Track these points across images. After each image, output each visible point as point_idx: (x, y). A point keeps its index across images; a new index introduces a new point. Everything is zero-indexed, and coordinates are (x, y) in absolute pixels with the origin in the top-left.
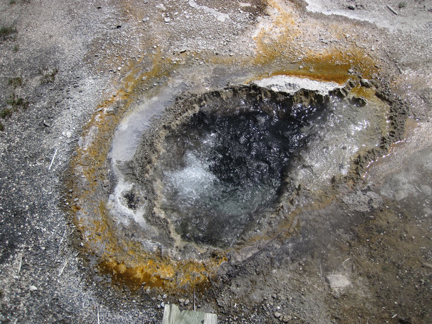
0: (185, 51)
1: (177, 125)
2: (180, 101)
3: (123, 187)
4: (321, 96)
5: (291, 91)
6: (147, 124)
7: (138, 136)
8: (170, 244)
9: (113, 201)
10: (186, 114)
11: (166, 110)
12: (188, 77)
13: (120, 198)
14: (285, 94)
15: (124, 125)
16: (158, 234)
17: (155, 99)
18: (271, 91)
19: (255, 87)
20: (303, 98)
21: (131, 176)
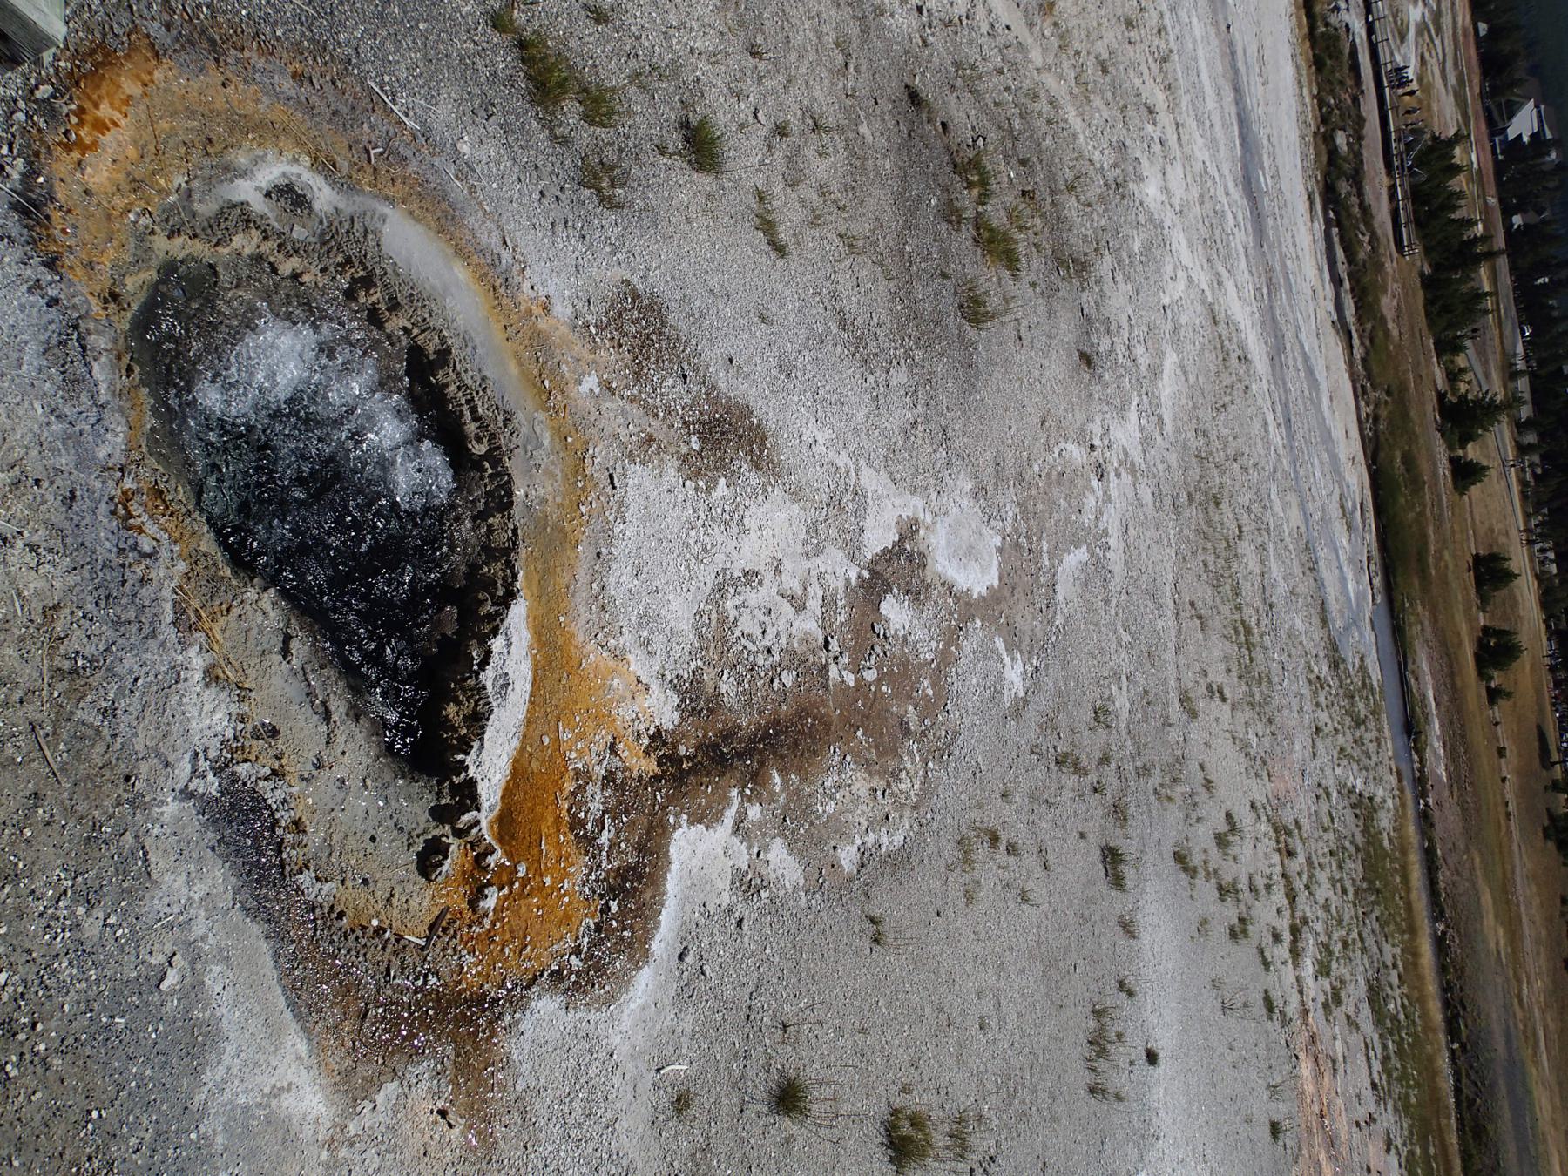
0: (614, 488)
1: (447, 385)
2: (500, 418)
3: (324, 196)
4: (467, 754)
5: (488, 677)
6: (460, 321)
7: (433, 288)
8: (167, 220)
9: (295, 160)
10: (468, 416)
11: (484, 379)
12: (552, 463)
13: (299, 176)
14: (485, 662)
15: (461, 273)
16: (197, 207)
17: (514, 369)
18: (495, 632)
19: (511, 595)
20: (467, 709)
21: (347, 225)
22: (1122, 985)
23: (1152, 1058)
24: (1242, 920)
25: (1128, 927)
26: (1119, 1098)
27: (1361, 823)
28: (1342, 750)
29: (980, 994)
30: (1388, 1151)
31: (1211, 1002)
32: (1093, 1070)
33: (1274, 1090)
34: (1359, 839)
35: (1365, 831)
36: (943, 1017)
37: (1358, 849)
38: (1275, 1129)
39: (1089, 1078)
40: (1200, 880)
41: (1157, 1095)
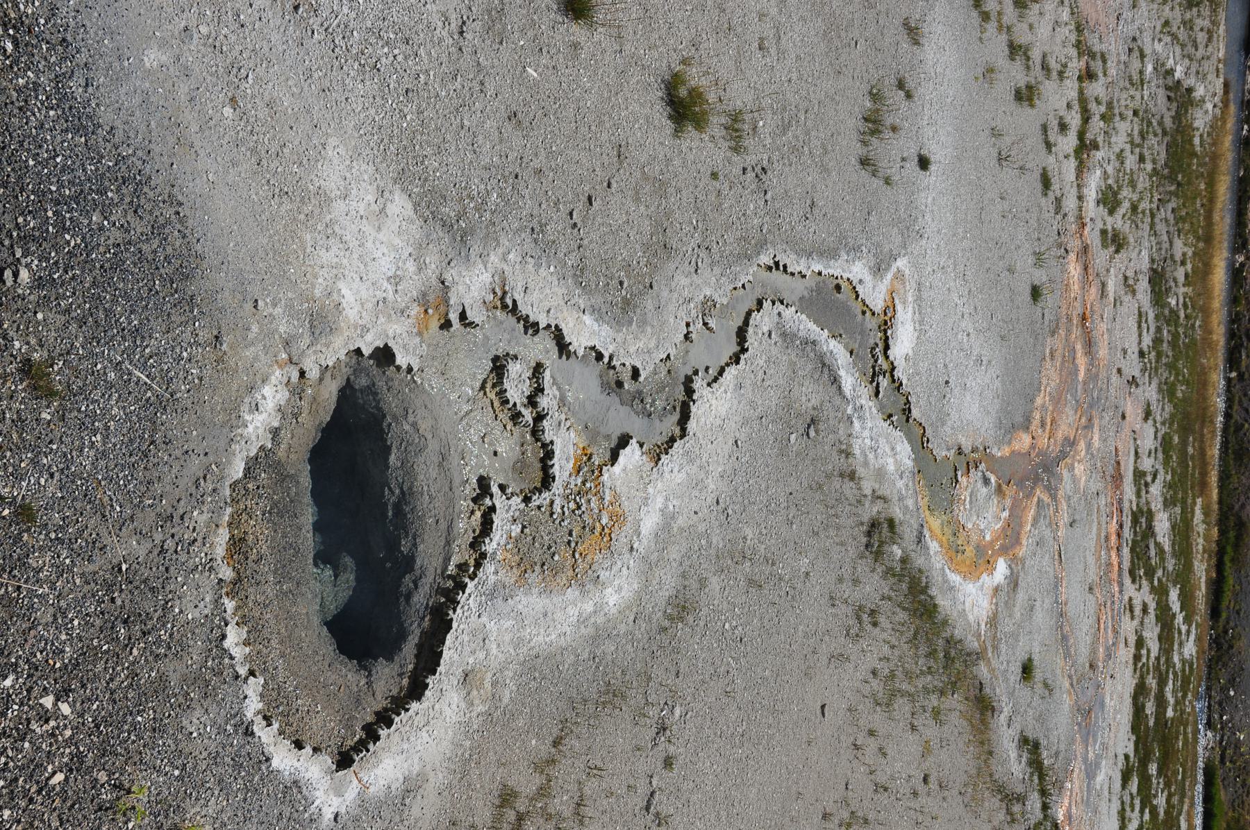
22: (901, 85)
23: (924, 163)
24: (1029, 87)
25: (913, 33)
26: (888, 181)
27: (1175, 104)
28: (1167, 23)
29: (762, 16)
30: (1146, 419)
31: (988, 153)
32: (864, 143)
33: (1039, 258)
34: (1168, 122)
35: (1177, 118)
36: (724, 19)
37: (1165, 133)
38: (1036, 293)
39: (860, 150)
40: (992, 26)
41: (925, 199)
